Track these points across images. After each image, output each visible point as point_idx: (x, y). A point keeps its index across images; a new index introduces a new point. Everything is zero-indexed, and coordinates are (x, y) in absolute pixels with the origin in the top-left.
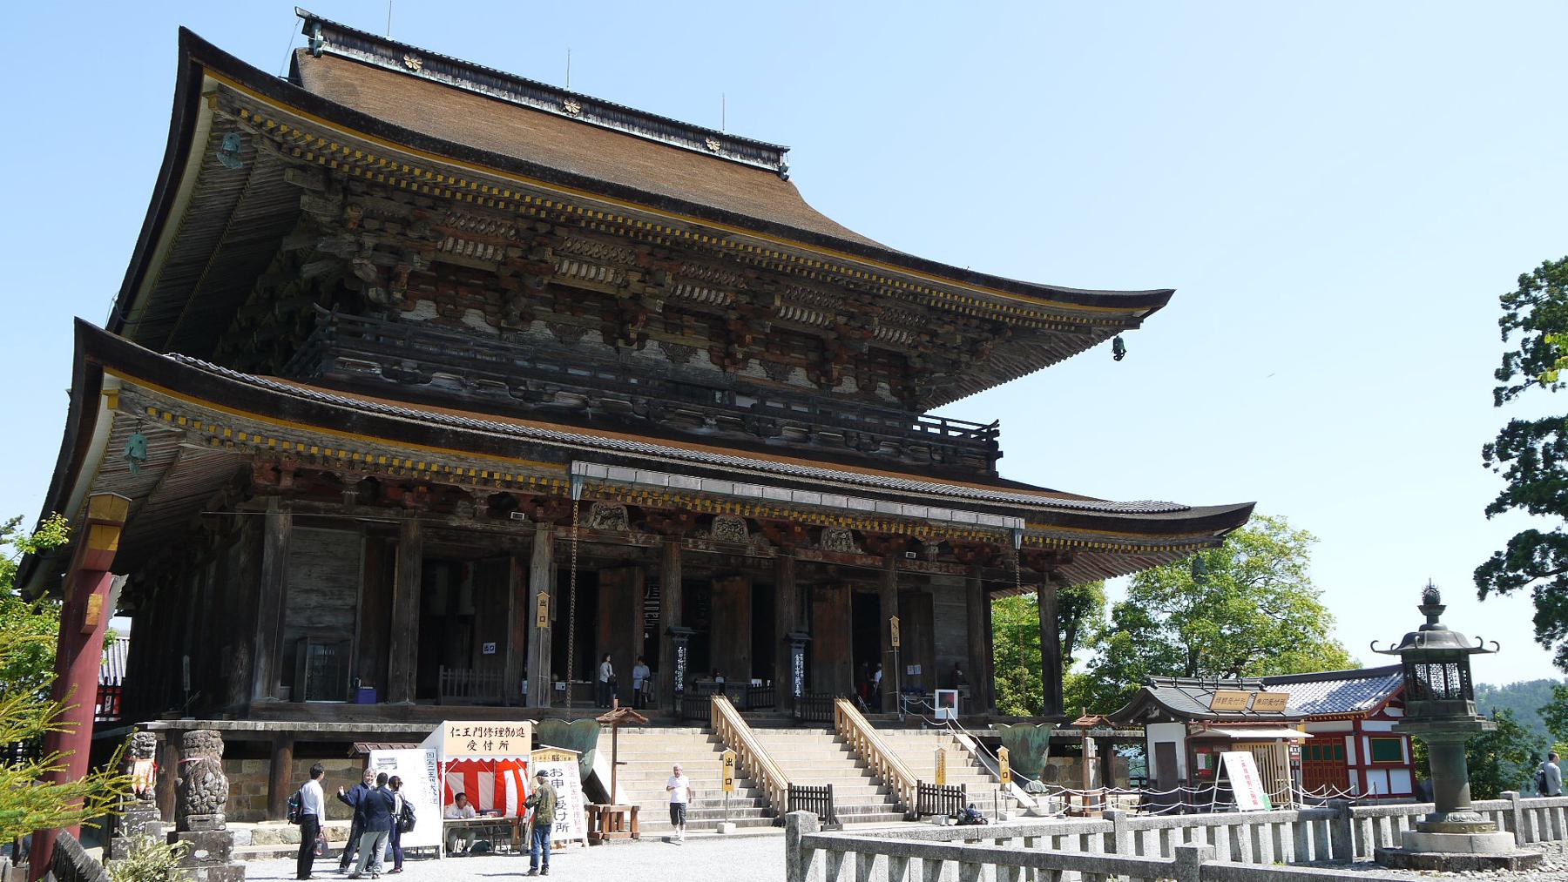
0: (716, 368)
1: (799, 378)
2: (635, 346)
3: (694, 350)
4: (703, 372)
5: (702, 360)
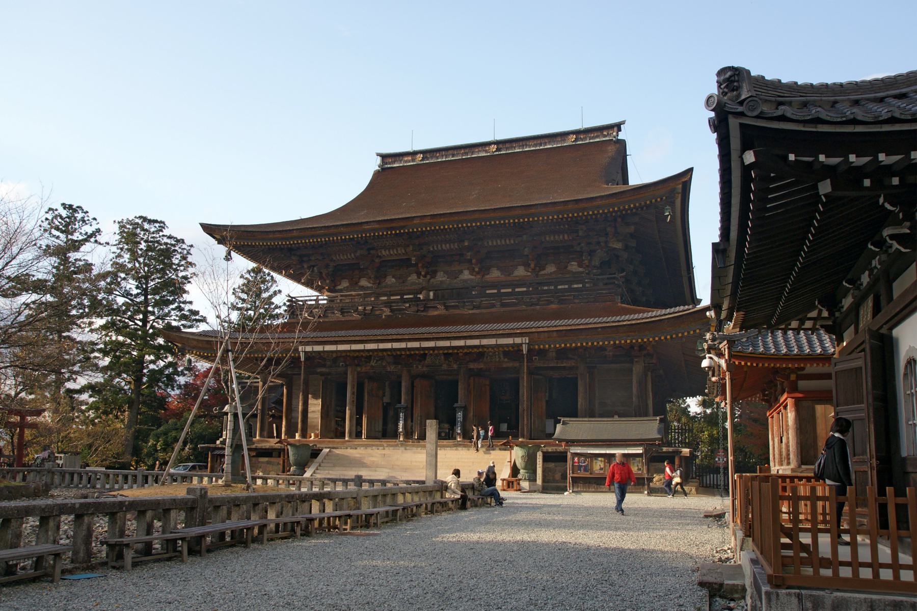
0: (472, 277)
1: (521, 272)
2: (428, 277)
3: (461, 272)
4: (466, 281)
5: (466, 275)
